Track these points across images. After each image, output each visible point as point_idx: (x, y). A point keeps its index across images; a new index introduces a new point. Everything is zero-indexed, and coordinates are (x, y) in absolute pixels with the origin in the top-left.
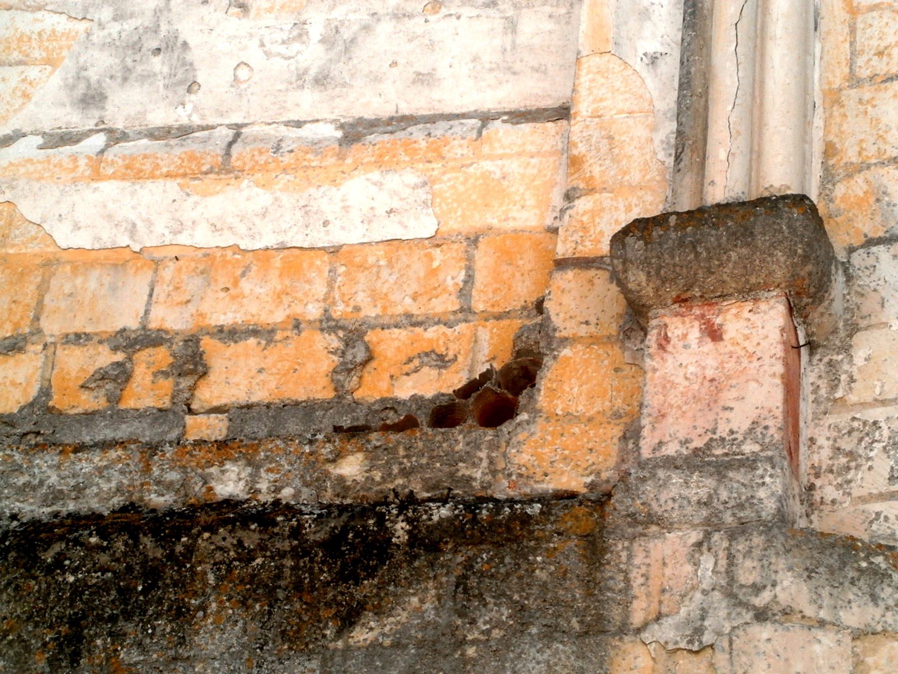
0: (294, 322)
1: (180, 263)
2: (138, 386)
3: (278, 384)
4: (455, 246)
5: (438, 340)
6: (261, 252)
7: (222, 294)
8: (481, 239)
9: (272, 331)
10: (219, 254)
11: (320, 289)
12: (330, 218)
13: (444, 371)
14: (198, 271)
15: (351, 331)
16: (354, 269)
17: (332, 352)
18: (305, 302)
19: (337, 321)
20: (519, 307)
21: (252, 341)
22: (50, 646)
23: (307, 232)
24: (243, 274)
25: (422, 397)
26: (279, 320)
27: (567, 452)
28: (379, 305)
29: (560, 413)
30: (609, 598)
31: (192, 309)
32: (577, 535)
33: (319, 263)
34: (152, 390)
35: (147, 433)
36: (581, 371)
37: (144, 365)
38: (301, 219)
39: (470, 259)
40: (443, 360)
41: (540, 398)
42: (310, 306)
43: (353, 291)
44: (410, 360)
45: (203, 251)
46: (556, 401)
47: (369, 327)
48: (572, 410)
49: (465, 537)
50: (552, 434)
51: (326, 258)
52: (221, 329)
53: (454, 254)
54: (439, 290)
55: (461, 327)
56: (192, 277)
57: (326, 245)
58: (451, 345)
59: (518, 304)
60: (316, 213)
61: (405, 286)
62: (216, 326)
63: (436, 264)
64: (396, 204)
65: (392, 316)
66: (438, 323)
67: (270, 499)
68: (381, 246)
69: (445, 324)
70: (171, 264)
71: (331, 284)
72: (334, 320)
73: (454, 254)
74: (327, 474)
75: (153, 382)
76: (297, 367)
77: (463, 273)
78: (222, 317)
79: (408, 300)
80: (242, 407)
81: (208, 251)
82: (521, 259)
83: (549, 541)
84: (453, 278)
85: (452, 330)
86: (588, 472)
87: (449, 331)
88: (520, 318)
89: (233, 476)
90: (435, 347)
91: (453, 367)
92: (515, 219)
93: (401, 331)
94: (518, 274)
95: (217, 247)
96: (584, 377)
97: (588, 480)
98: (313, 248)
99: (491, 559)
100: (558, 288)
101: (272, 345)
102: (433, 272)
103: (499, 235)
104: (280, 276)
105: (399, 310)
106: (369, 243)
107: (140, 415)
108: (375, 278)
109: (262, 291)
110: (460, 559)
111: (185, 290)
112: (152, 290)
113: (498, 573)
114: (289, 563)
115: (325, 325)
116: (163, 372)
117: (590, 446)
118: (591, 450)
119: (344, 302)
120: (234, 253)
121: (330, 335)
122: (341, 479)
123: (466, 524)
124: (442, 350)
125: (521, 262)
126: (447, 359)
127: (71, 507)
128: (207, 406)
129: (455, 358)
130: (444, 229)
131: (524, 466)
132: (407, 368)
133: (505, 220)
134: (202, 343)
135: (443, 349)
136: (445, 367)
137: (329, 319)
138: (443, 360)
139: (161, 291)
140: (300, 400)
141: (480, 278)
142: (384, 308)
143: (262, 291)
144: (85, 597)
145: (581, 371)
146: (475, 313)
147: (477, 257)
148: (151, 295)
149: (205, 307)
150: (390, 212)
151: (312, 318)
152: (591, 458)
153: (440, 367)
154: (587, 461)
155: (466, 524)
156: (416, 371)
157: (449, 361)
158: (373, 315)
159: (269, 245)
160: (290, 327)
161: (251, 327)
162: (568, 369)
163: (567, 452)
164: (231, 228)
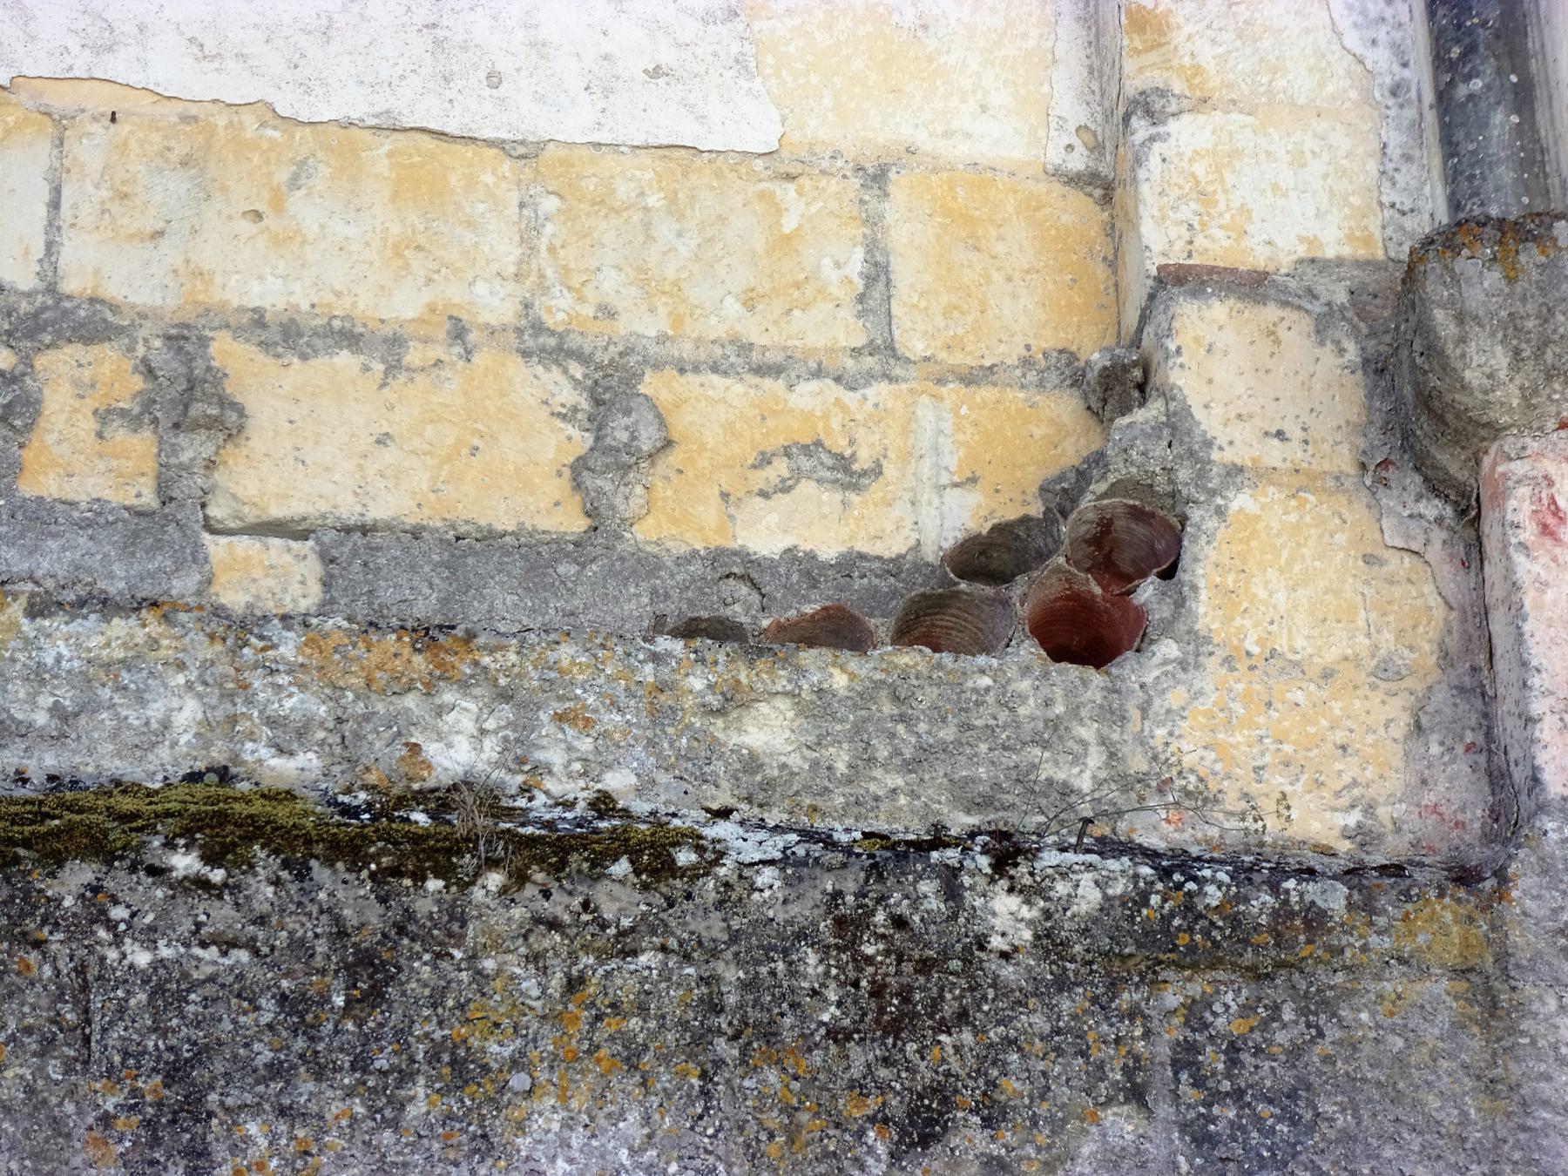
0: (448, 325)
1: (123, 129)
2: (59, 442)
3: (434, 479)
4: (833, 185)
5: (826, 417)
6: (332, 129)
7: (246, 227)
8: (892, 175)
9: (396, 342)
10: (221, 121)
11: (504, 248)
12: (504, 66)
13: (853, 497)
14: (173, 157)
15: (599, 367)
16: (585, 207)
17: (563, 417)
18: (470, 275)
19: (561, 336)
20: (1012, 360)
21: (345, 359)
22: (120, 1124)
23: (449, 94)
24: (294, 183)
25: (811, 556)
26: (410, 314)
27: (1288, 748)
28: (662, 311)
29: (1256, 650)
30: (1546, 1124)
31: (169, 252)
32: (1442, 966)
33: (489, 178)
34: (101, 456)
35: (119, 569)
36: (1285, 554)
37: (66, 388)
38: (428, 58)
39: (873, 221)
40: (847, 470)
41: (1202, 610)
42: (481, 288)
43: (592, 263)
44: (765, 460)
45: (179, 107)
46: (1238, 622)
47: (645, 361)
48: (1281, 644)
49: (1175, 948)
50: (1247, 699)
51: (507, 167)
52: (259, 320)
53: (833, 205)
54: (809, 290)
55: (879, 391)
56: (160, 171)
57: (504, 135)
58: (860, 434)
59: (1011, 353)
60: (465, 49)
61: (721, 269)
62: (242, 310)
63: (789, 224)
64: (666, 57)
65: (698, 342)
66: (818, 373)
67: (580, 792)
68: (644, 158)
69: (838, 379)
70: (95, 128)
71: (528, 236)
72: (552, 333)
73: (833, 205)
74: (714, 746)
75: (100, 435)
76: (476, 442)
77: (859, 254)
78: (256, 288)
79: (733, 307)
80: (347, 530)
81: (194, 110)
82: (1001, 238)
83: (1378, 977)
84: (838, 265)
85: (858, 395)
86: (1345, 801)
87: (850, 398)
88: (1023, 387)
89: (468, 724)
90: (822, 436)
91: (876, 491)
92: (968, 136)
93: (728, 381)
94: (997, 277)
95: (215, 101)
96: (1297, 568)
97: (1353, 818)
98: (474, 139)
99: (1247, 1009)
100: (1197, 340)
101: (403, 377)
102: (786, 244)
103: (935, 171)
104: (394, 198)
105: (715, 328)
106: (615, 146)
107: (97, 519)
108: (641, 238)
109: (350, 231)
110: (1172, 999)
111: (146, 204)
112: (57, 191)
113: (1270, 1042)
114: (731, 974)
115: (530, 343)
116: (123, 413)
117: (1339, 736)
118: (1343, 748)
119: (569, 289)
120: (263, 125)
121: (548, 369)
122: (752, 763)
123: (1172, 915)
124: (839, 444)
125: (1000, 248)
126: (856, 467)
127: (49, 760)
128: (251, 515)
129: (877, 471)
130: (796, 136)
131: (1192, 771)
132: (761, 478)
133: (948, 134)
134: (213, 349)
135: (844, 442)
136: (855, 487)
137: (538, 328)
138: (847, 470)
139: (80, 197)
140: (499, 527)
141: (905, 273)
142: (678, 321)
143: (350, 231)
144: (190, 1009)
145: (1285, 554)
146: (908, 361)
147: (889, 219)
148: (55, 205)
149: (208, 254)
150: (656, 72)
151: (494, 321)
152: (1349, 769)
153: (846, 487)
154: (1340, 773)
155: (1172, 915)
156: (785, 488)
157: (864, 473)
158: (652, 333)
159: (354, 115)
160: (442, 335)
161: (337, 324)
162: (1254, 543)
163: (1288, 748)
164: (242, 57)
